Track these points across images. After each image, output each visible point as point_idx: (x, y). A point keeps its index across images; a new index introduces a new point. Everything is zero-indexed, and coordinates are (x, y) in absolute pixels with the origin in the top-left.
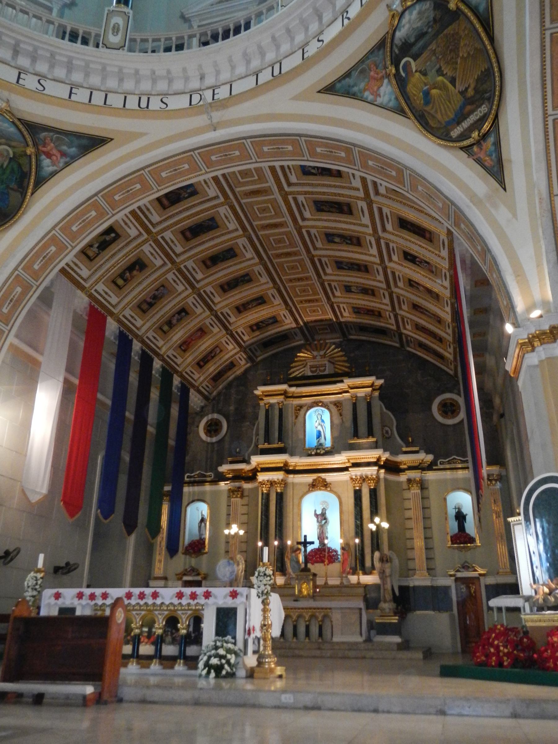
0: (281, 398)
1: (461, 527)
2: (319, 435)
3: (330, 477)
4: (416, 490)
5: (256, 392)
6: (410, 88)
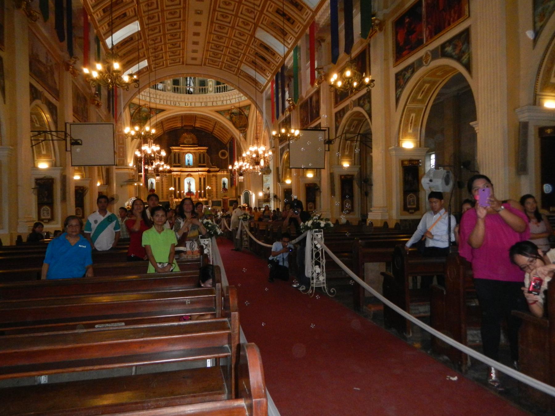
0: (179, 150)
1: (224, 186)
2: (188, 161)
3: (192, 173)
4: (214, 178)
5: (171, 148)
6: (233, 119)
